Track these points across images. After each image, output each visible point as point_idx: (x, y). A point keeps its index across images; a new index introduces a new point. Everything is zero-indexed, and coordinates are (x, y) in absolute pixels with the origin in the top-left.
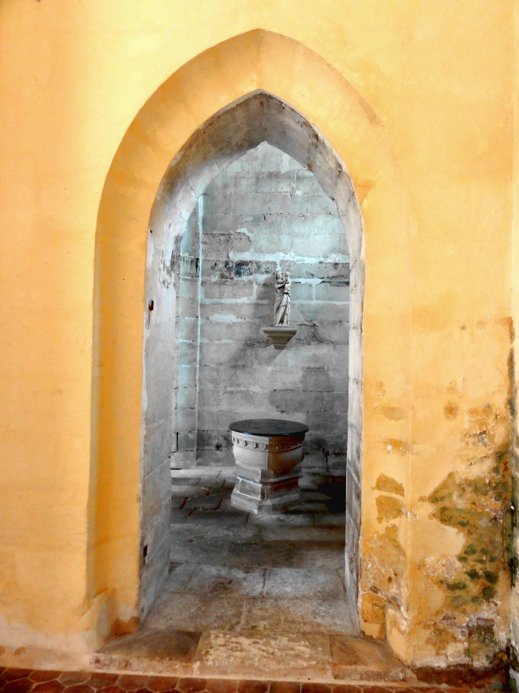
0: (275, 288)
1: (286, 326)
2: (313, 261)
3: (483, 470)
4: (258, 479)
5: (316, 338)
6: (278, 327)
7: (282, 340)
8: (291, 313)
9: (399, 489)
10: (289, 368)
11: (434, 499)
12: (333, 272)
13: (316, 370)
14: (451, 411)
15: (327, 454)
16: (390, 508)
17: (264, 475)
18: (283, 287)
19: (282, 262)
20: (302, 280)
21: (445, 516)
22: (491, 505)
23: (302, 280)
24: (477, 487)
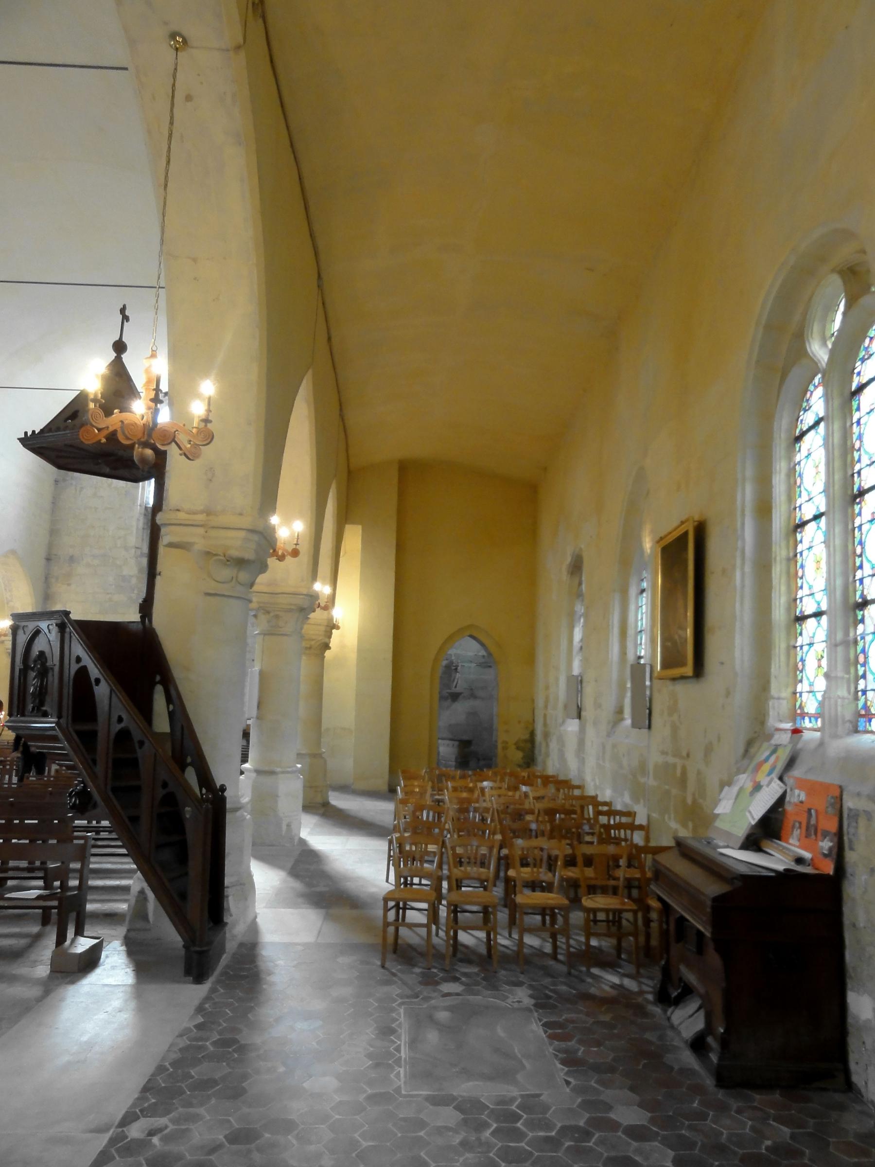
0: (451, 669)
1: (458, 690)
2: (471, 654)
3: (527, 736)
4: (453, 760)
5: (473, 696)
6: (454, 690)
7: (455, 697)
8: (460, 682)
9: (507, 743)
10: (458, 712)
11: (516, 744)
12: (483, 660)
13: (473, 714)
14: (519, 722)
15: (479, 760)
16: (505, 748)
17: (456, 758)
18: (456, 669)
19: (455, 655)
20: (466, 665)
21: (518, 748)
22: (529, 745)
23: (466, 665)
24: (526, 741)
